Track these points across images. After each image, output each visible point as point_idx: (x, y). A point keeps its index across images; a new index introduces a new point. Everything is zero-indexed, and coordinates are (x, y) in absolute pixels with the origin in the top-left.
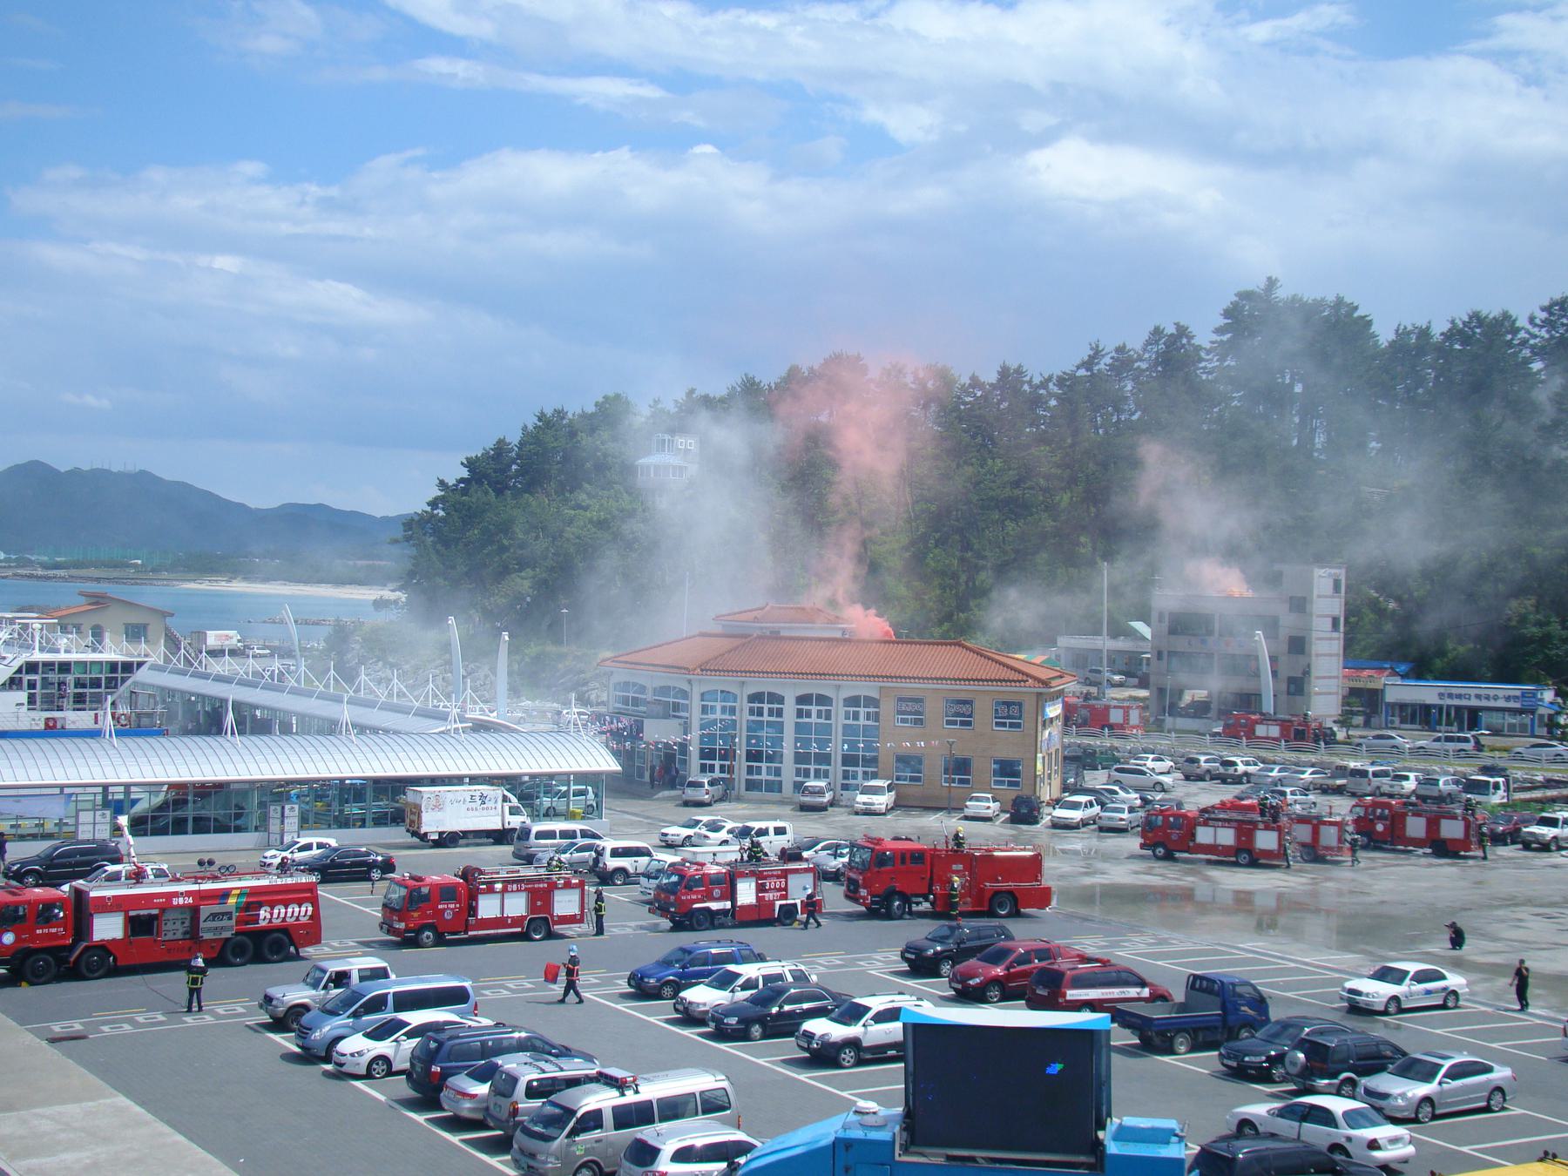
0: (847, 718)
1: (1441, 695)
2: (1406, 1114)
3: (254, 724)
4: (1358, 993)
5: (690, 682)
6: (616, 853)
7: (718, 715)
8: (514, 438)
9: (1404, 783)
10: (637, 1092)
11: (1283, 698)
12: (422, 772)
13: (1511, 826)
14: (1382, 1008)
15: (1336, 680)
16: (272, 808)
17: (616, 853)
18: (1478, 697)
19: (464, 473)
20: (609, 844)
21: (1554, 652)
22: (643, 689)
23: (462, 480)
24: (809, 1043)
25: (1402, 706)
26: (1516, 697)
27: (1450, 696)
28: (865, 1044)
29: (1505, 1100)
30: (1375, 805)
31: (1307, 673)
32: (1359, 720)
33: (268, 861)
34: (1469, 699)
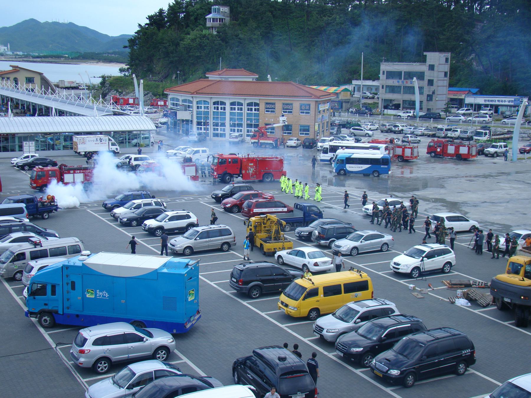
0: (248, 110)
1: (485, 101)
2: (347, 253)
3: (61, 113)
5: (192, 97)
6: (136, 159)
7: (203, 110)
8: (166, 8)
9: (456, 133)
10: (41, 246)
11: (425, 102)
12: (97, 130)
13: (481, 148)
15: (445, 96)
16: (24, 143)
17: (136, 159)
18: (499, 101)
19: (148, 21)
20: (133, 156)
22: (178, 100)
23: (147, 24)
24: (145, 228)
25: (471, 105)
26: (513, 101)
27: (488, 101)
28: (165, 228)
29: (388, 247)
30: (438, 141)
31: (433, 93)
33: (13, 162)
34: (495, 102)
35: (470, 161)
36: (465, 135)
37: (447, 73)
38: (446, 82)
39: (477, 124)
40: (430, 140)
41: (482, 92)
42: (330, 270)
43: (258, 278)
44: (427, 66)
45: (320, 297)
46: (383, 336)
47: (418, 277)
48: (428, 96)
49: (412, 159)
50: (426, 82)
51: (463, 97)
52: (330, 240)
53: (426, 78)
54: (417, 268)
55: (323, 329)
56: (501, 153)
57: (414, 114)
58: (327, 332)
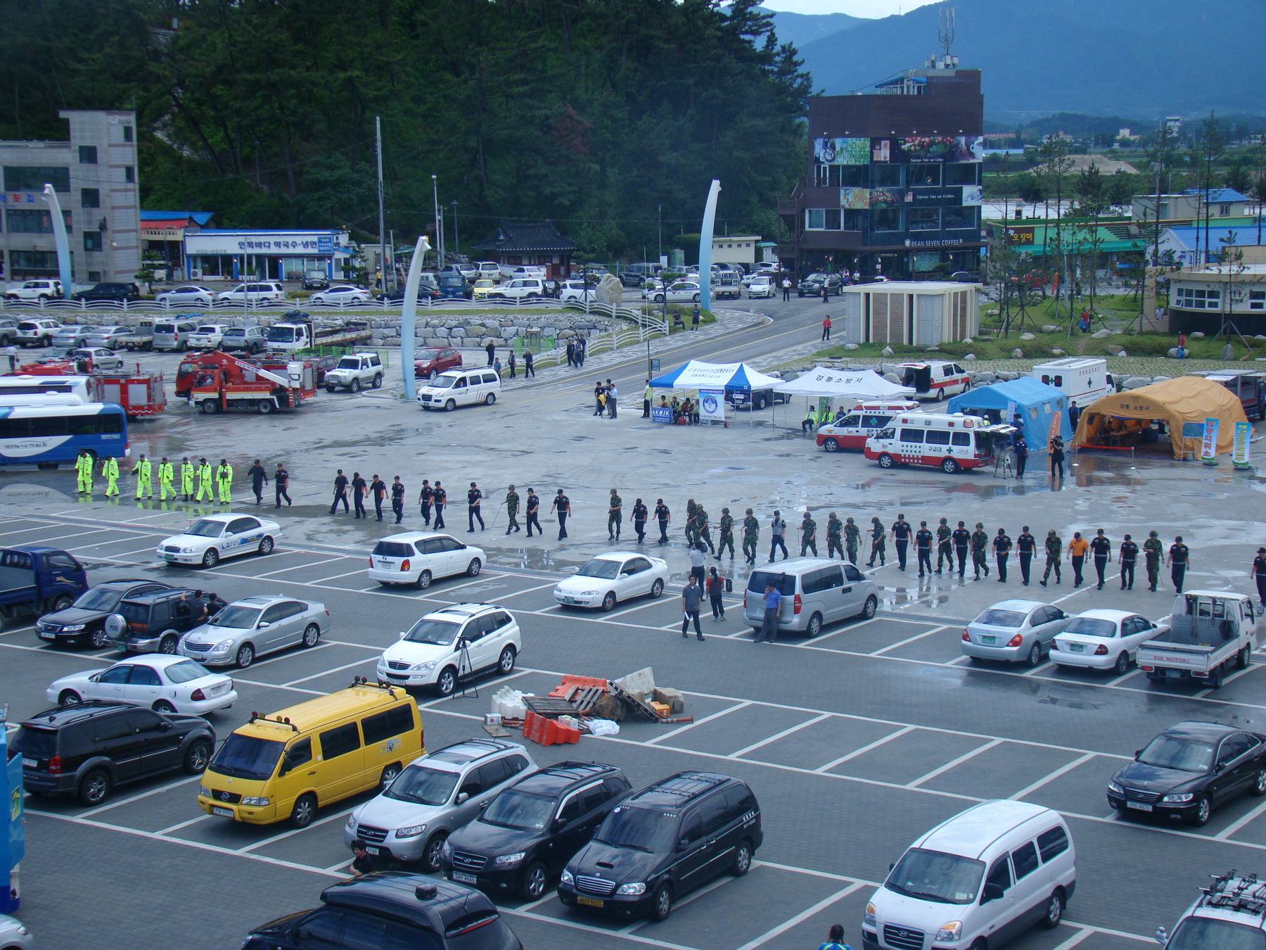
1: (241, 244)
4: (177, 550)
9: (210, 335)
14: (201, 562)
15: (133, 235)
18: (278, 244)
21: (345, 196)
27: (250, 244)
29: (319, 635)
31: (103, 227)
32: (160, 274)
35: (305, 405)
36: (239, 341)
37: (133, 169)
38: (133, 198)
39: (254, 309)
40: (182, 357)
41: (220, 223)
42: (229, 707)
43: (101, 746)
44: (74, 151)
45: (317, 762)
46: (557, 817)
47: (453, 692)
48: (88, 235)
49: (152, 414)
50: (76, 196)
51: (178, 236)
52: (163, 635)
53: (77, 184)
54: (450, 669)
55: (386, 832)
56: (366, 379)
57: (58, 291)
58: (397, 836)
